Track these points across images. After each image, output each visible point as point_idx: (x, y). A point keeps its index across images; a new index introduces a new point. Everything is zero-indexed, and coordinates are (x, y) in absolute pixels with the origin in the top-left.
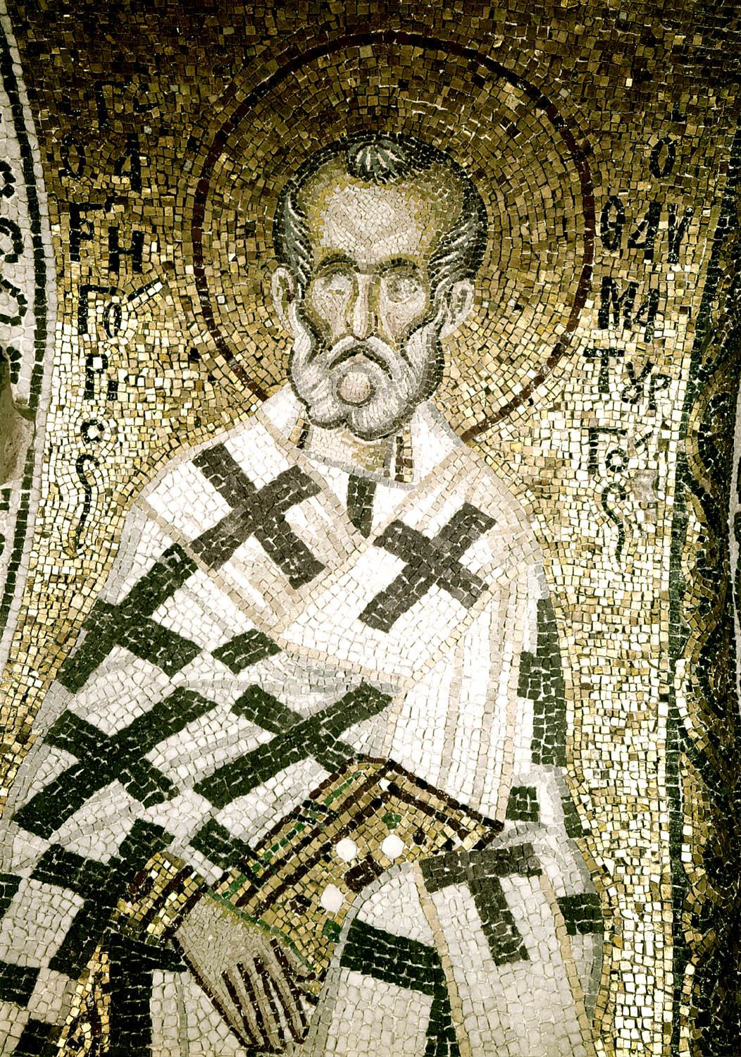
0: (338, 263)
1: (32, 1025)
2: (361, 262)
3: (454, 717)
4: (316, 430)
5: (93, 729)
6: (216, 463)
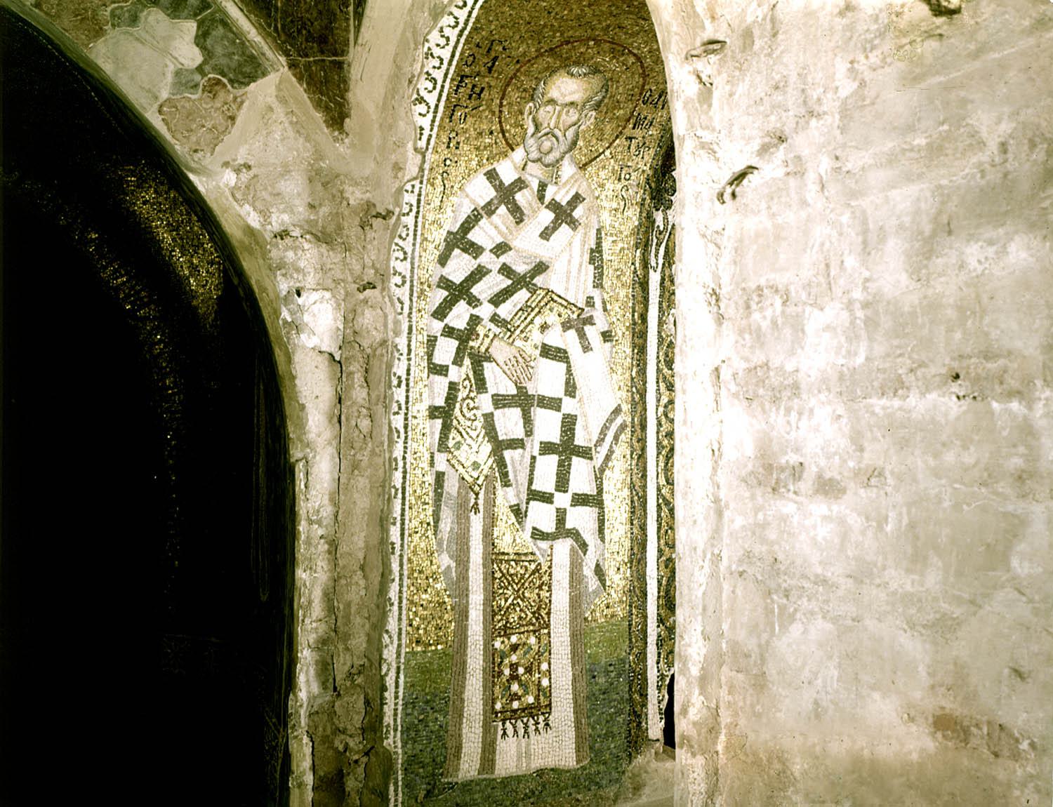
0: (552, 101)
1: (451, 383)
2: (559, 102)
3: (569, 272)
4: (530, 164)
5: (451, 282)
6: (492, 176)
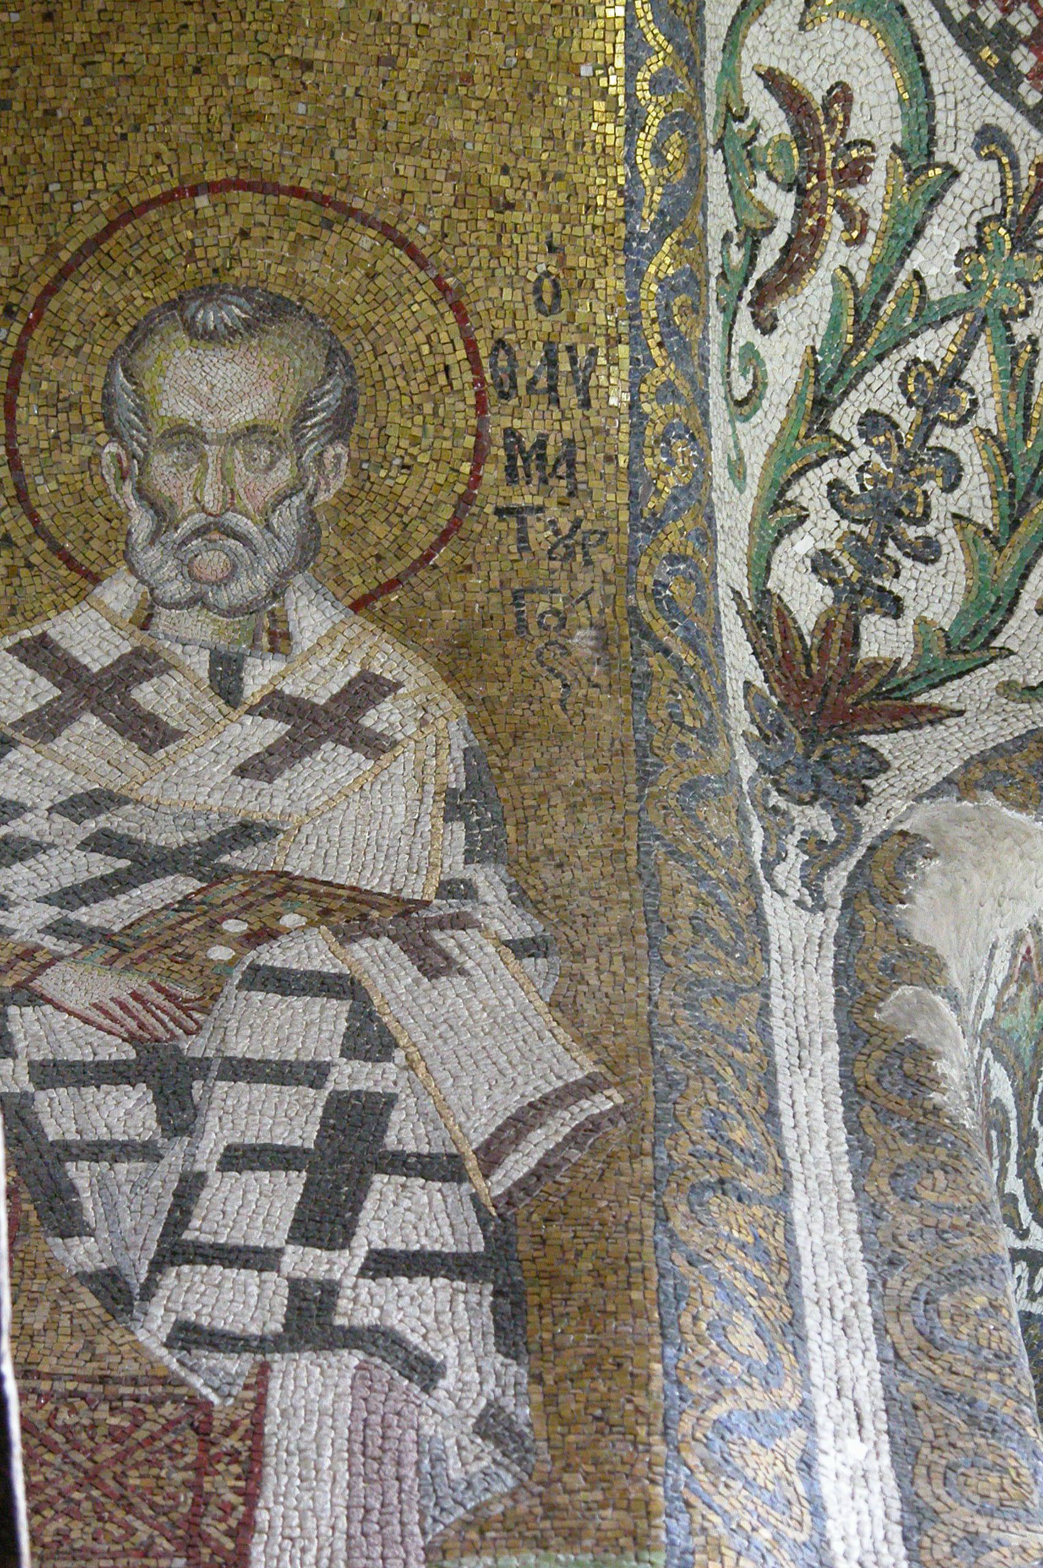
2: (210, 431)
